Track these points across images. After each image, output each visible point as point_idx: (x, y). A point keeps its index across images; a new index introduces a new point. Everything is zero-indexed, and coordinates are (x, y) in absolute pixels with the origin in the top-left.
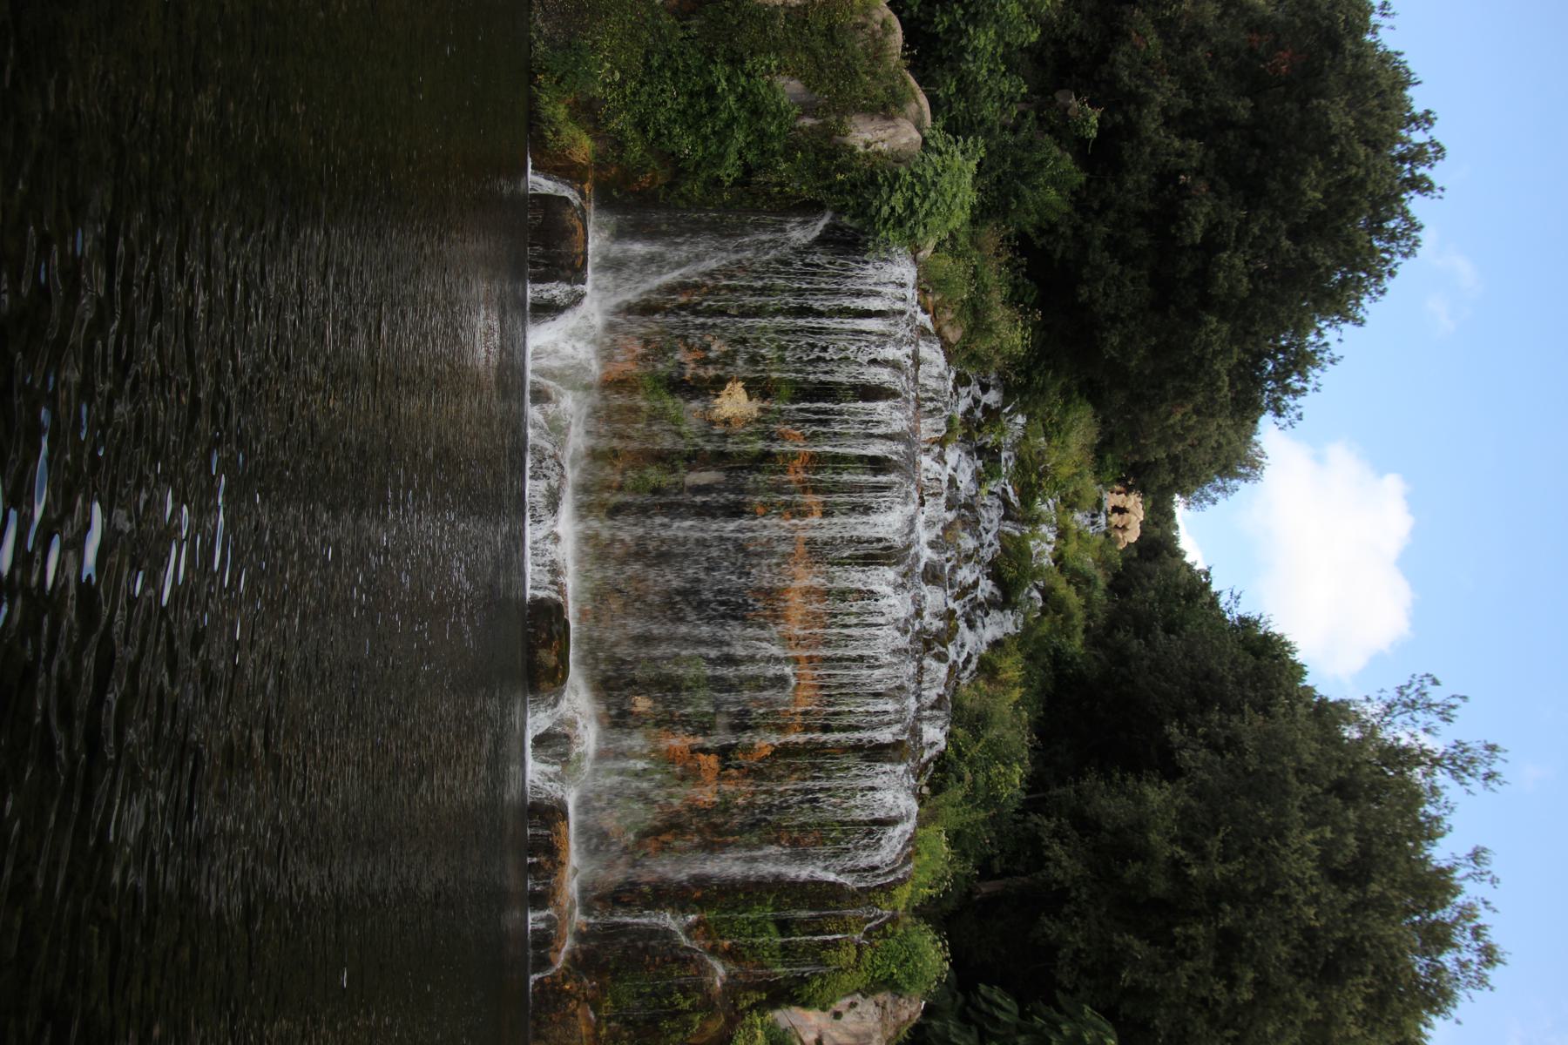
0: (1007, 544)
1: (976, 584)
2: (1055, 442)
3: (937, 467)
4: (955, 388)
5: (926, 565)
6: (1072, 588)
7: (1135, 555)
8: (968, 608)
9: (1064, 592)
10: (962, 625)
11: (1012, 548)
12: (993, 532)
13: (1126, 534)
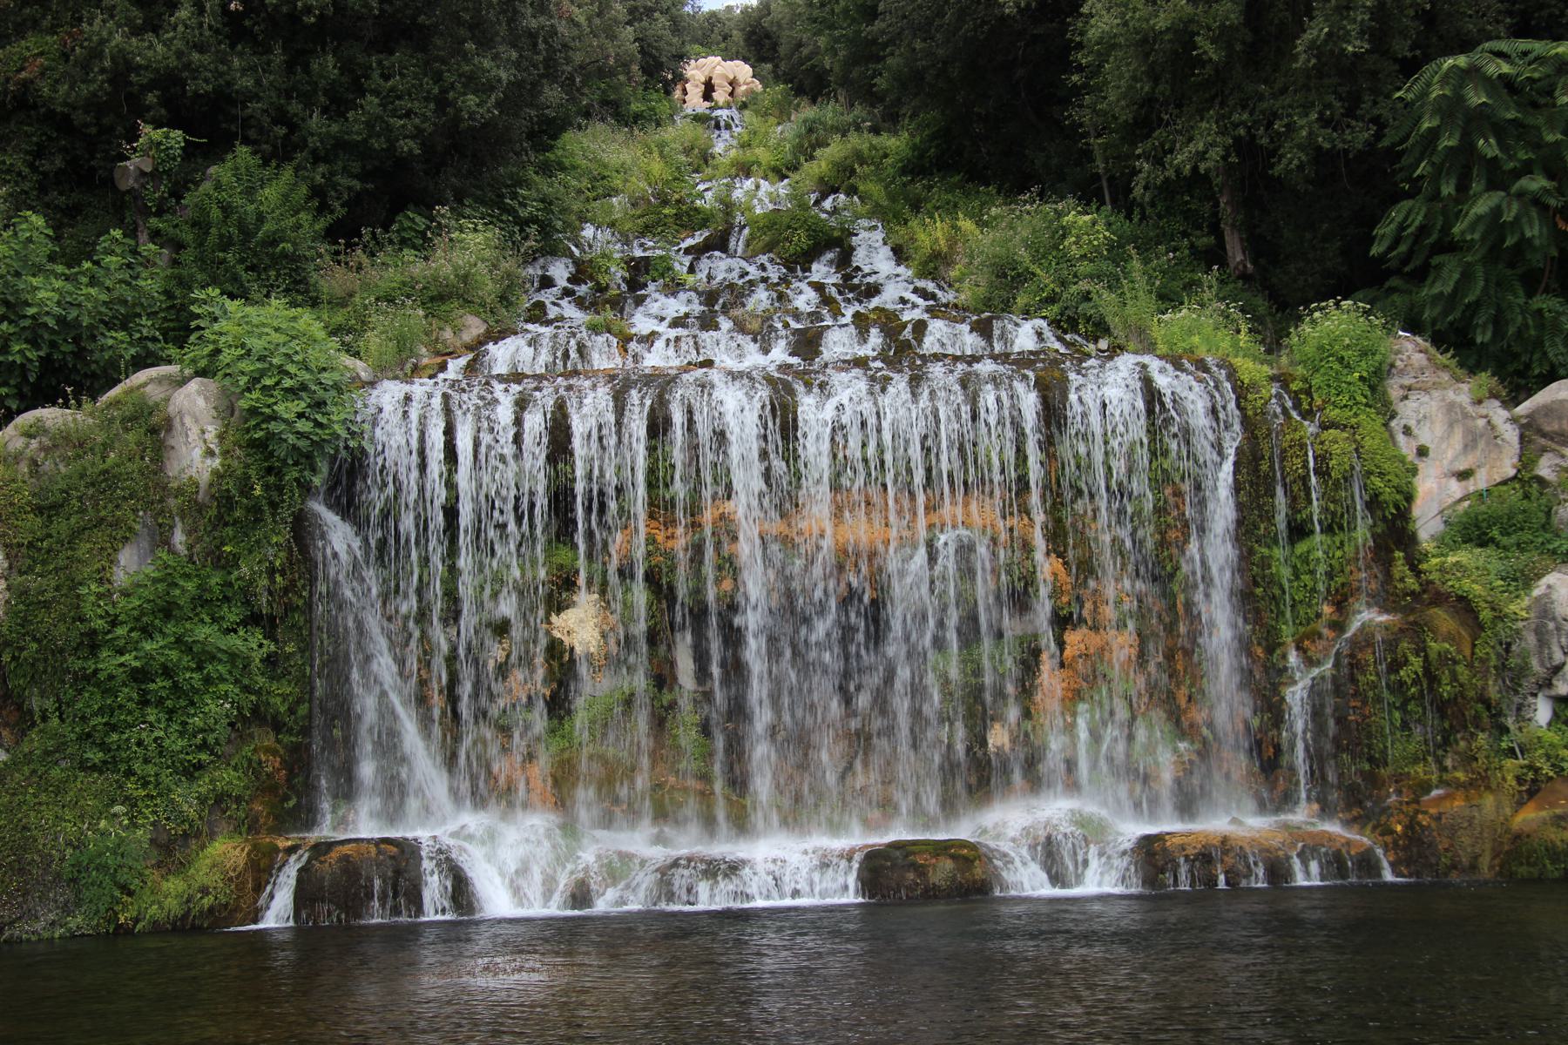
1: (819, 287)
2: (617, 182)
3: (659, 344)
5: (791, 354)
6: (818, 152)
7: (769, 66)
8: (850, 296)
9: (823, 164)
10: (875, 302)
11: (766, 238)
12: (744, 264)
13: (741, 81)
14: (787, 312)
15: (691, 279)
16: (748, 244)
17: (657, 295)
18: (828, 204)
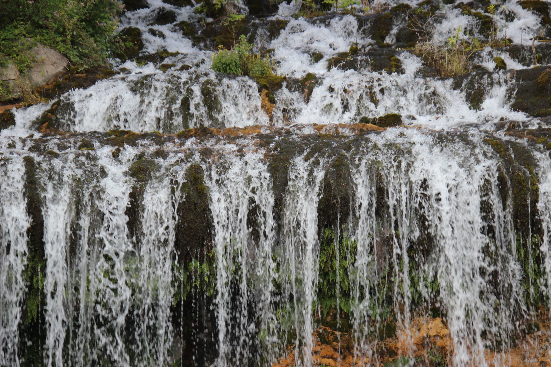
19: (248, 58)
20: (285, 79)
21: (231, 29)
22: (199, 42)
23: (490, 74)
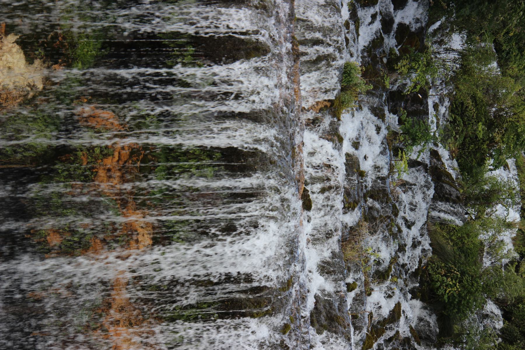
0: (443, 241)
4: (354, 15)
11: (449, 247)
12: (419, 224)
14: (366, 284)
15: (403, 165)
16: (443, 224)
17: (384, 132)
18: (491, 307)
19: (355, 90)
20: (339, 120)
21: (378, 77)
22: (368, 52)
23: (344, 279)
